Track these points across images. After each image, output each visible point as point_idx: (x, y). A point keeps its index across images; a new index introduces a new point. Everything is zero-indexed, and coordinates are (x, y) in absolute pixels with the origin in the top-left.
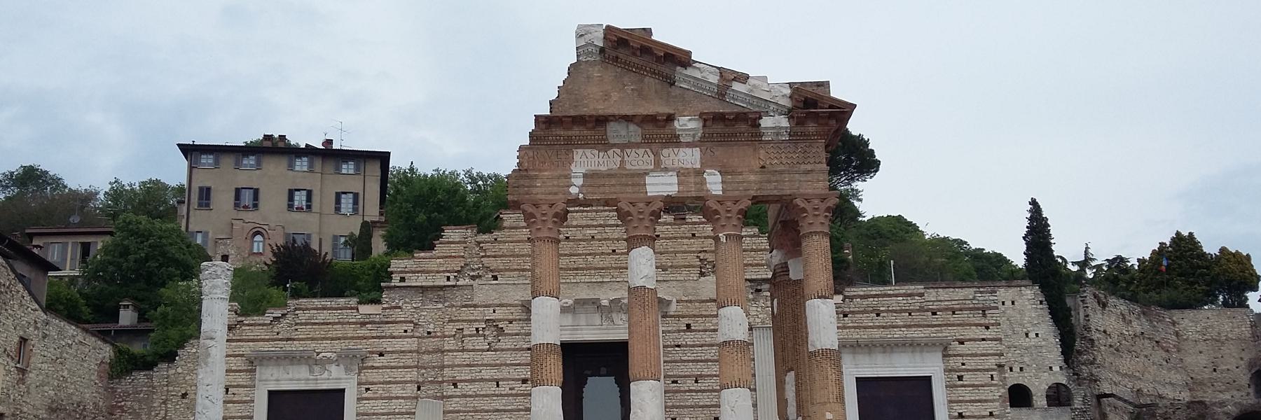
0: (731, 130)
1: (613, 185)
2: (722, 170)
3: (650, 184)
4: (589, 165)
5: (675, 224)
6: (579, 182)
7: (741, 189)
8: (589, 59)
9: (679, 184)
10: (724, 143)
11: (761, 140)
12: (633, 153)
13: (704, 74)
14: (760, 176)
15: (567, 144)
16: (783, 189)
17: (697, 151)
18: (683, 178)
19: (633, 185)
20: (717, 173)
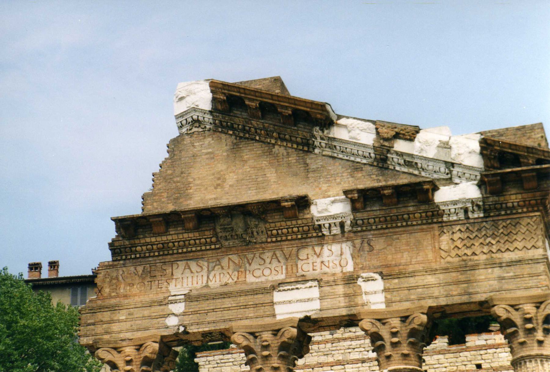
0: (395, 211)
1: (229, 309)
2: (384, 273)
3: (280, 303)
4: (195, 282)
5: (449, 352)
6: (179, 308)
7: (413, 297)
8: (196, 129)
9: (321, 298)
10: (387, 231)
11: (442, 222)
12: (257, 260)
13: (353, 134)
14: (441, 276)
15: (163, 255)
16: (477, 293)
17: (347, 248)
18: (327, 289)
19: (256, 305)
20: (377, 276)
